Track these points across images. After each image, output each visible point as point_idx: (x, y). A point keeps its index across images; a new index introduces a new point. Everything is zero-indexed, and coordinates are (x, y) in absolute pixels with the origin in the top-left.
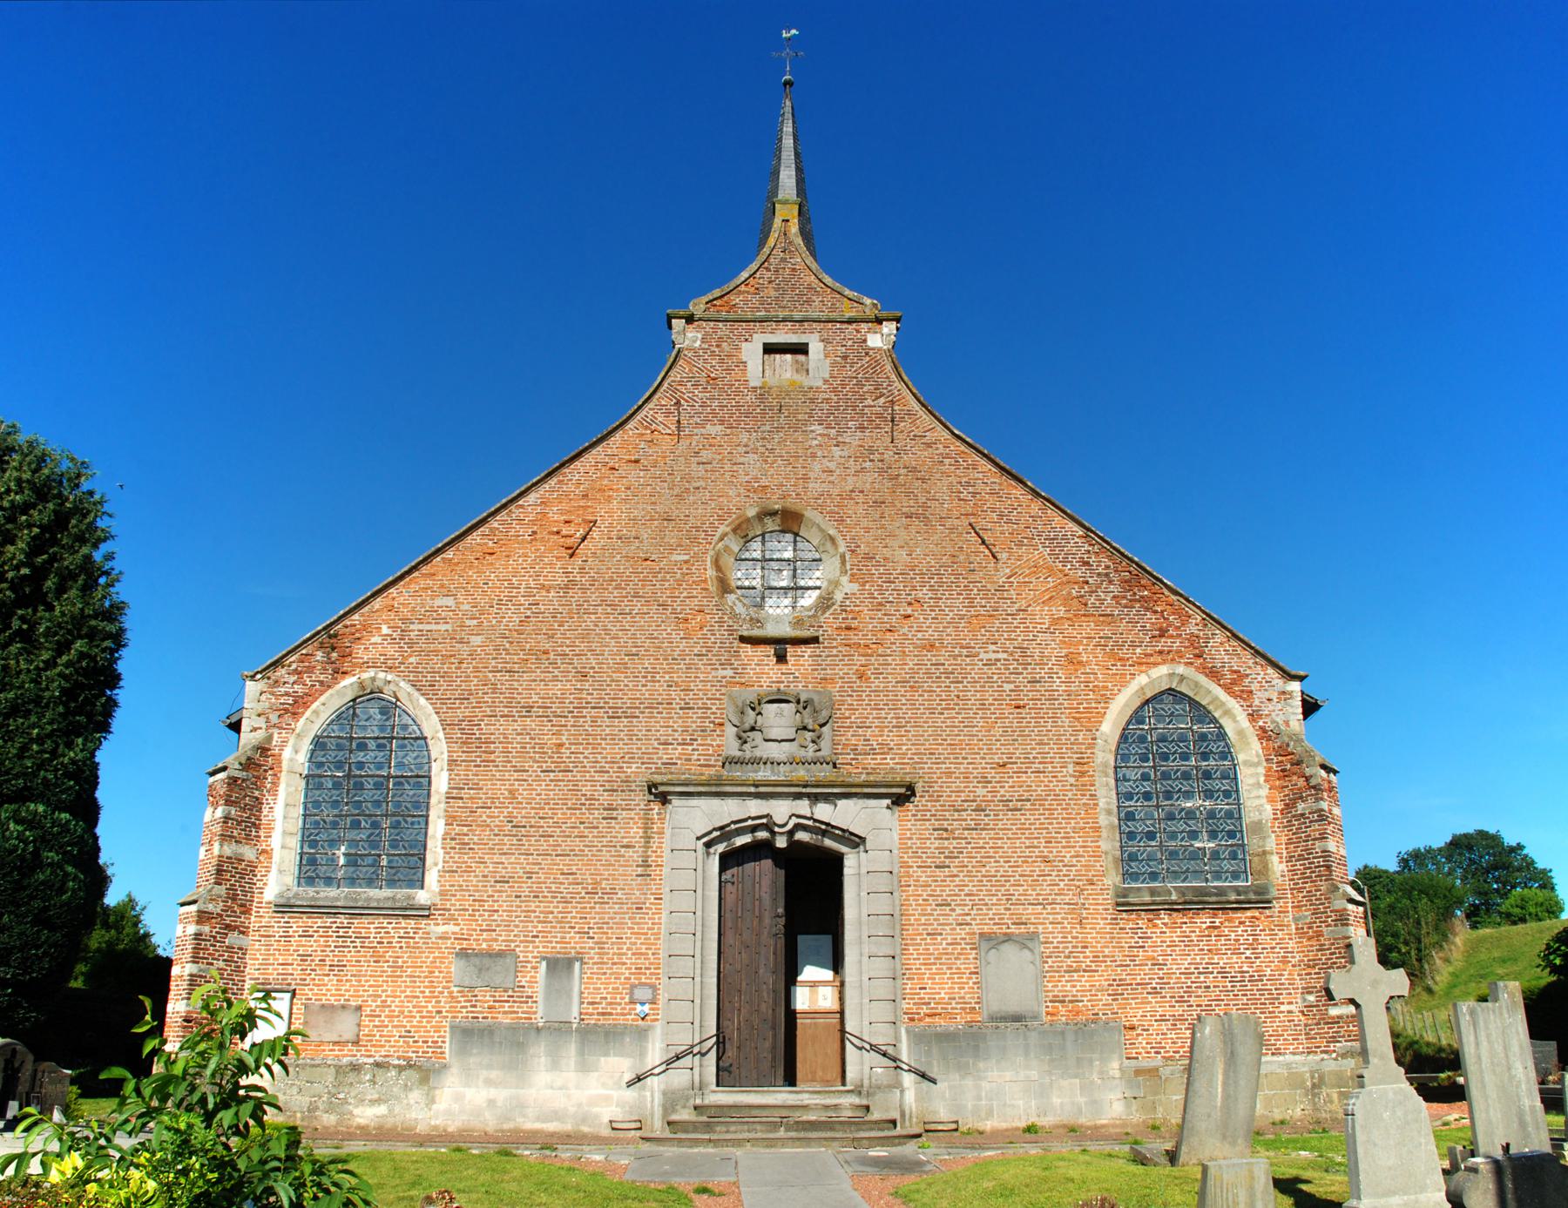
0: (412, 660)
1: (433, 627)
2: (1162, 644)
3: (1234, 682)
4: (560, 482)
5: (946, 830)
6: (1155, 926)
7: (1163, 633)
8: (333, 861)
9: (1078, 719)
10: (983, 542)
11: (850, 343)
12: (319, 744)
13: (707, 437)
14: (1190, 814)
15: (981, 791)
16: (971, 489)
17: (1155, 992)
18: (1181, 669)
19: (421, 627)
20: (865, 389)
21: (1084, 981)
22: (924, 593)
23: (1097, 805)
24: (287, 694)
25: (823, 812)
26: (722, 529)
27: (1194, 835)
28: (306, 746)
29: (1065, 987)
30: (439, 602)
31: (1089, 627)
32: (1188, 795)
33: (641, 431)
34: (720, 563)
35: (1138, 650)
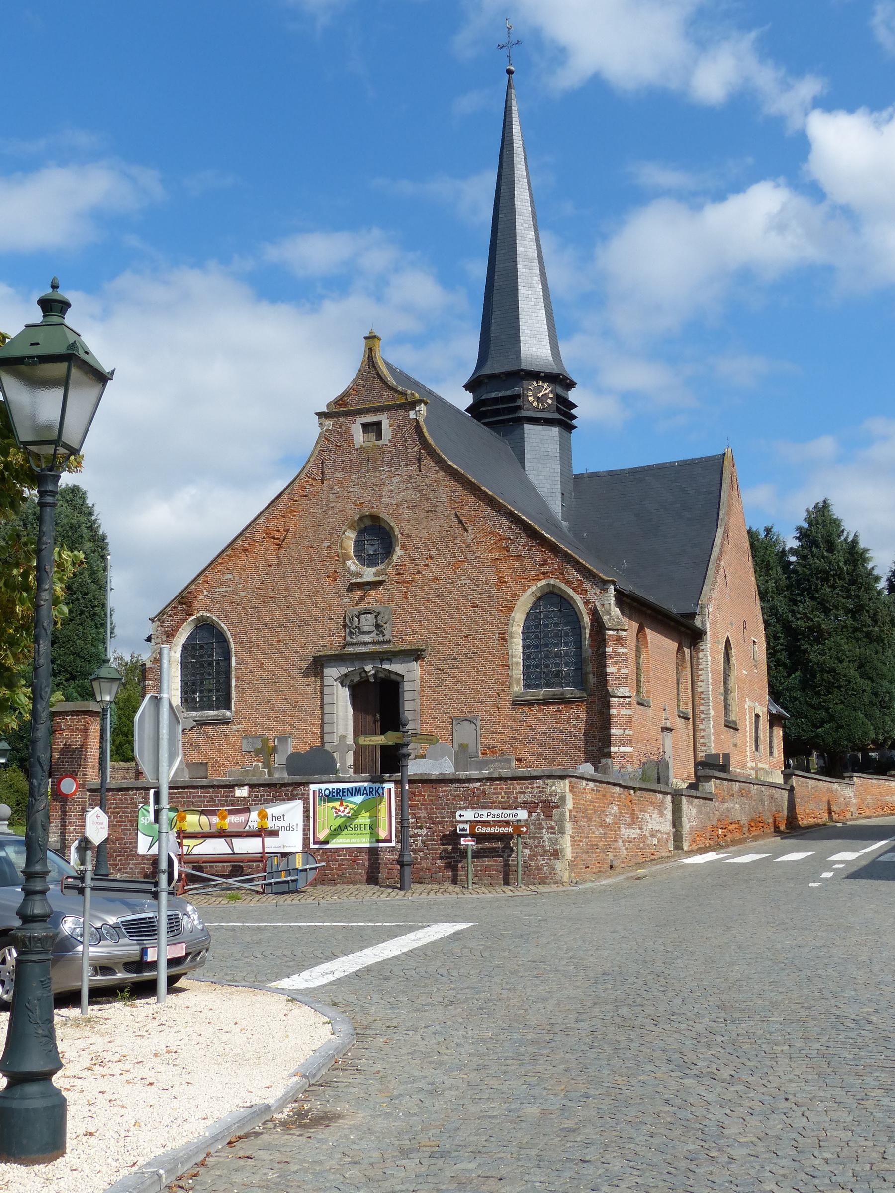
0: (217, 606)
1: (225, 589)
2: (543, 569)
3: (578, 586)
4: (273, 510)
5: (440, 669)
6: (532, 710)
7: (544, 563)
8: (195, 699)
9: (501, 611)
10: (460, 522)
11: (401, 417)
12: (185, 647)
13: (336, 479)
14: (557, 655)
15: (456, 650)
16: (457, 494)
17: (530, 742)
18: (552, 581)
19: (219, 590)
20: (408, 443)
21: (498, 738)
22: (433, 553)
23: (508, 653)
24: (168, 626)
25: (386, 666)
26: (344, 528)
27: (557, 665)
28: (179, 649)
29: (491, 741)
30: (227, 577)
31: (509, 563)
32: (556, 645)
33: (307, 479)
34: (344, 545)
35: (532, 573)
